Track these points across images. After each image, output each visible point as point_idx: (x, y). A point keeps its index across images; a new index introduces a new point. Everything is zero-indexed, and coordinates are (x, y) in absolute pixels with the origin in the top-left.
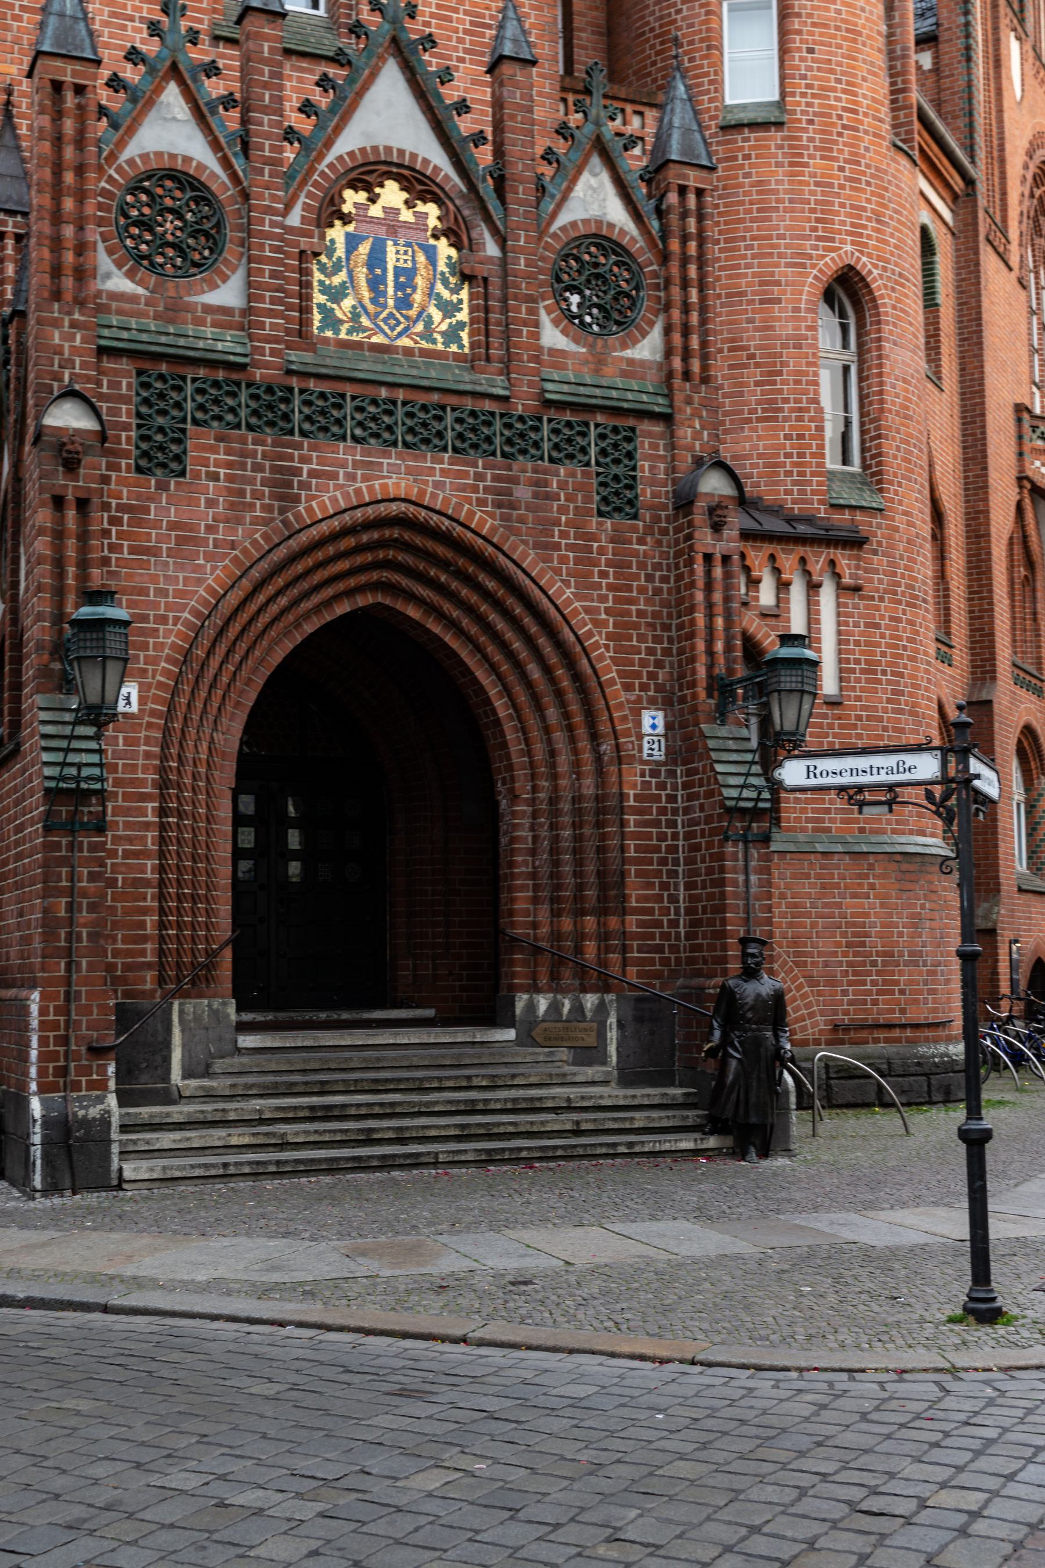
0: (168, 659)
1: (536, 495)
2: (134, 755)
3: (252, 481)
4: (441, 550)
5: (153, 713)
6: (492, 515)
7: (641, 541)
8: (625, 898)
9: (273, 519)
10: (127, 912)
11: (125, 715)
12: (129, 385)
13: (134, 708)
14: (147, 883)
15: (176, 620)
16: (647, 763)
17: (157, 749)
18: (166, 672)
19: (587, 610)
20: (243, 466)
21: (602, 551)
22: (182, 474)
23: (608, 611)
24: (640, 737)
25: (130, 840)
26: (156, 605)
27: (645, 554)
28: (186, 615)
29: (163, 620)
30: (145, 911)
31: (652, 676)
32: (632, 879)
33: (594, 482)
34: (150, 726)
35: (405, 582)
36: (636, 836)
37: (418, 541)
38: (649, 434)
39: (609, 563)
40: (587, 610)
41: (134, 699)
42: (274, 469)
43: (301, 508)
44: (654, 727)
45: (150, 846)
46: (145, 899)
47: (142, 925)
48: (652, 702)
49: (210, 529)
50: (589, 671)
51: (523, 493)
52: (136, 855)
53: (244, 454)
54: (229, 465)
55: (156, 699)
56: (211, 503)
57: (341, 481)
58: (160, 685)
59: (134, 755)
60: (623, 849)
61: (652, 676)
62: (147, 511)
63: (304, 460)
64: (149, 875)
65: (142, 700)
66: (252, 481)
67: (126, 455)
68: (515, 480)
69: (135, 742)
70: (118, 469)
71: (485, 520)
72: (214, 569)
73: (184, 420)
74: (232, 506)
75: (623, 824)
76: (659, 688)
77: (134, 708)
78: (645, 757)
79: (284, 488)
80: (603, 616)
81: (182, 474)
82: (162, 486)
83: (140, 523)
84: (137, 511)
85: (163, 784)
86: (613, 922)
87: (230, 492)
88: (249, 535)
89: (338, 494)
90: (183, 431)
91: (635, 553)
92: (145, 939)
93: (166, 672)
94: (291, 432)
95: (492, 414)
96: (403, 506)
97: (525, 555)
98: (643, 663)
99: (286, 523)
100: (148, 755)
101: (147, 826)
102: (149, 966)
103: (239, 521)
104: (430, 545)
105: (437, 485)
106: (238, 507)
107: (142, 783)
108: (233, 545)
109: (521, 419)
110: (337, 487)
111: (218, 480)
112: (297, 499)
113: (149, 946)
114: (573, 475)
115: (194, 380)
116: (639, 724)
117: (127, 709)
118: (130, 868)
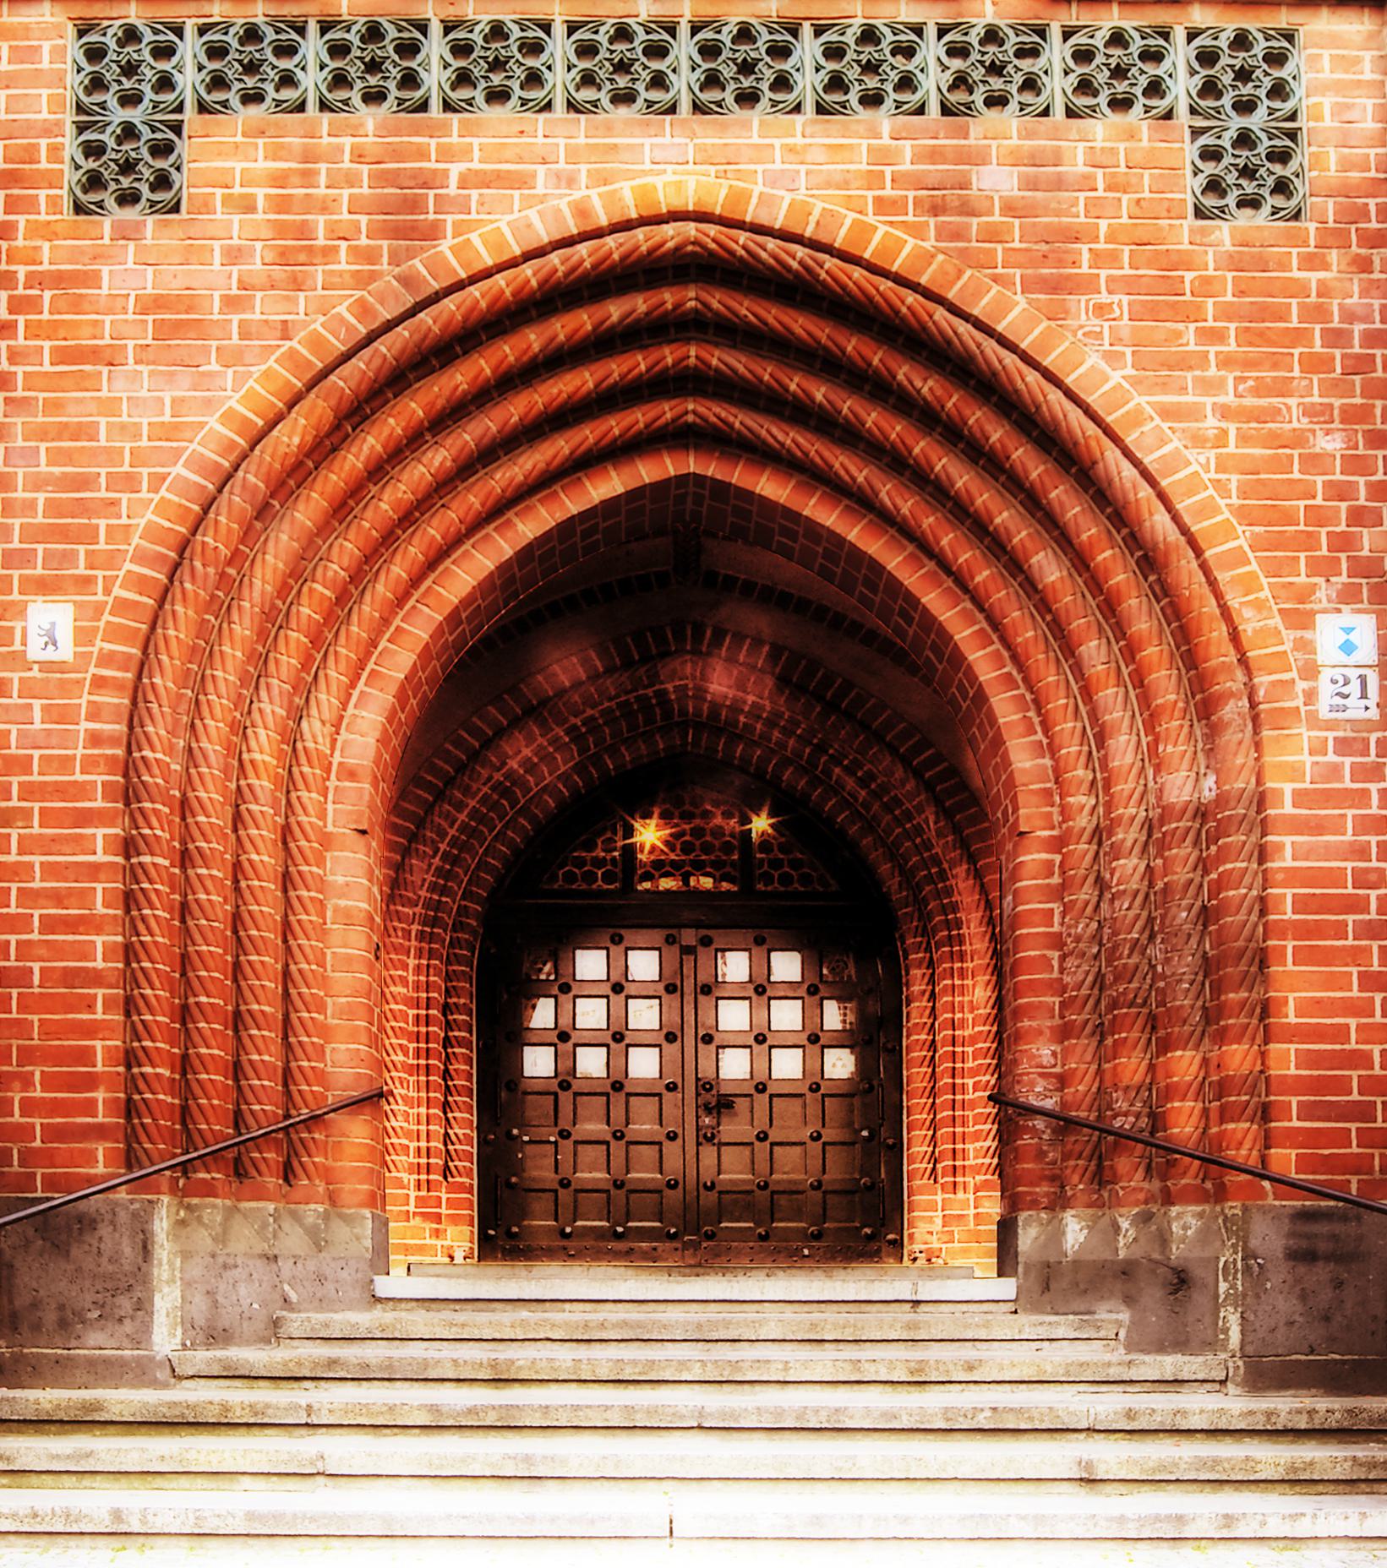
0: (140, 557)
1: (1031, 184)
2: (67, 740)
3: (325, 207)
4: (800, 324)
5: (106, 659)
6: (917, 231)
7: (1312, 262)
8: (1266, 1009)
9: (373, 276)
10: (48, 1030)
11: (47, 666)
12: (58, 53)
13: (65, 651)
14: (96, 978)
15: (157, 481)
16: (1330, 725)
17: (121, 728)
18: (141, 583)
19: (1166, 413)
20: (308, 178)
21: (1206, 287)
22: (176, 209)
23: (1225, 413)
24: (1311, 671)
25: (58, 898)
26: (113, 455)
27: (1324, 291)
28: (179, 470)
29: (129, 482)
30: (91, 1029)
31: (1342, 542)
32: (1287, 967)
33: (1191, 151)
34: (99, 683)
35: (740, 419)
36: (1294, 877)
37: (746, 308)
38: (1334, 41)
39: (1226, 313)
40: (1166, 413)
41: (65, 636)
42: (381, 179)
43: (445, 246)
44: (1348, 648)
45: (100, 909)
46: (91, 1008)
47: (86, 1056)
48: (1349, 596)
49: (230, 303)
50: (1173, 534)
51: (996, 181)
52: (71, 925)
53: (309, 156)
54: (279, 180)
55: (113, 633)
56: (234, 256)
57: (540, 190)
58: (122, 606)
59: (67, 740)
60: (1264, 906)
61: (1342, 542)
62: (93, 279)
63: (446, 154)
64: (99, 964)
65: (83, 636)
66: (325, 207)
67: (52, 180)
68: (978, 158)
69: (64, 715)
70: (30, 205)
71: (904, 243)
72: (239, 381)
73: (180, 109)
74: (284, 258)
75: (1263, 854)
76: (1359, 568)
77: (65, 651)
78: (1324, 713)
79: (406, 216)
80: (1212, 422)
81: (176, 209)
82: (124, 233)
83: (77, 305)
84: (72, 283)
85: (129, 794)
86: (1238, 1056)
87: (281, 230)
88: (328, 312)
89: (533, 214)
90: (177, 128)
91: (1301, 290)
92: (91, 1082)
93: (141, 583)
94: (423, 107)
95: (918, 30)
96: (691, 229)
97: (1004, 307)
98: (1317, 517)
99: (407, 281)
100: (95, 739)
101: (94, 871)
102: (100, 1132)
103: (297, 285)
104: (774, 315)
105: (773, 180)
106: (295, 253)
107: (83, 791)
108: (285, 331)
109: (992, 36)
110: (528, 203)
111: (251, 208)
112: (433, 233)
113: (100, 1095)
114: (1132, 135)
115: (202, 30)
116: (1305, 646)
117: (50, 655)
118: (58, 951)
